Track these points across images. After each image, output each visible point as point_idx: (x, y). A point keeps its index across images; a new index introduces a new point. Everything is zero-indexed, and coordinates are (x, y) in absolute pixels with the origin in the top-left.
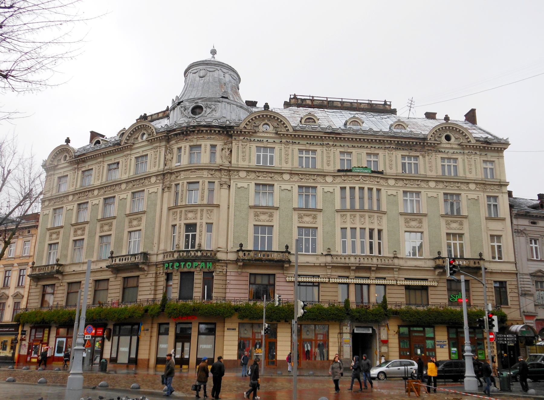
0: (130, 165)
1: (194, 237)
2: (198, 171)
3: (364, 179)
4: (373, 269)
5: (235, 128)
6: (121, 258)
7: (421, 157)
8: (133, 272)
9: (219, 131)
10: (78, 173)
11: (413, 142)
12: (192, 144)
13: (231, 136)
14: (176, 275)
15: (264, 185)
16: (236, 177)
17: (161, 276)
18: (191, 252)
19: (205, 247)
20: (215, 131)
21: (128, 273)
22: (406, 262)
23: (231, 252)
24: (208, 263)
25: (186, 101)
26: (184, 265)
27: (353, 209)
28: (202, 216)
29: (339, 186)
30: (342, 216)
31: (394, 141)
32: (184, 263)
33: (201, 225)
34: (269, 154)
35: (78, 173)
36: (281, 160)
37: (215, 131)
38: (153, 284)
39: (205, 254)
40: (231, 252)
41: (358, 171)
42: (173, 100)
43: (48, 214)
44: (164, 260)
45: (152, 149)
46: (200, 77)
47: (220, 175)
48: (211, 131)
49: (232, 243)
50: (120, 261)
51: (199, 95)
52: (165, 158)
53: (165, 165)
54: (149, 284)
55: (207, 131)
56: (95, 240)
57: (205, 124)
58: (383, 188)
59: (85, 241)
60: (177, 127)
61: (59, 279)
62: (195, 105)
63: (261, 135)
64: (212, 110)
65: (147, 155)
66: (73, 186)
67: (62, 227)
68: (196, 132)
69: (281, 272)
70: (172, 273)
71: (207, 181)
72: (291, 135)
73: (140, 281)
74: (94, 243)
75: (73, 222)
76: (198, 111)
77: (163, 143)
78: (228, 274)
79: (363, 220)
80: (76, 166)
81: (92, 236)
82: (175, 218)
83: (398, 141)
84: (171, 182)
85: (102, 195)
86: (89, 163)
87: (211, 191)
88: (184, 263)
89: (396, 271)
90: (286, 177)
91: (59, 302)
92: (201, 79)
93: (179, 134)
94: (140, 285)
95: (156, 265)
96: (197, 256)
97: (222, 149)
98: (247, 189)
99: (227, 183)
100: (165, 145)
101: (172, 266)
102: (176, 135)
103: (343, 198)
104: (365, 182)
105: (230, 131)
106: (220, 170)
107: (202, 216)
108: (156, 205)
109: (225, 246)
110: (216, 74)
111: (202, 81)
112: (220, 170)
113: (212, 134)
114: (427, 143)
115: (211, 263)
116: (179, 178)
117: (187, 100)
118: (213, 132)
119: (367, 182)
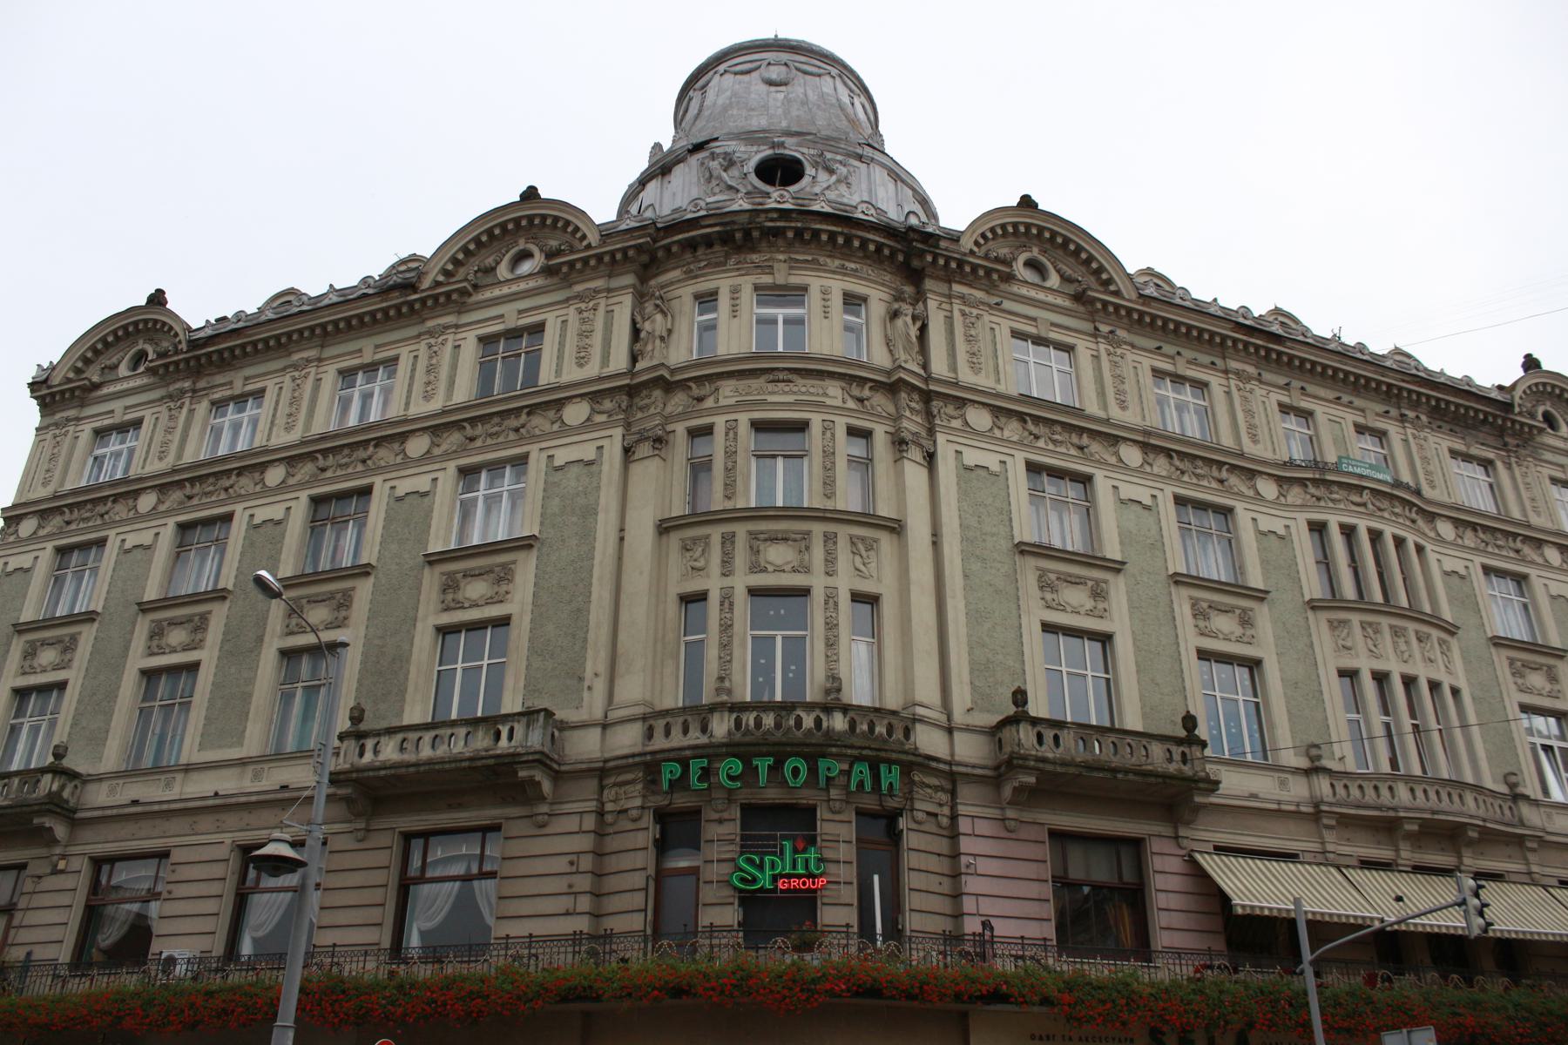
0: (454, 367)
1: (795, 650)
2: (800, 381)
3: (1378, 504)
4: (1473, 834)
5: (943, 244)
6: (413, 736)
7: (1499, 464)
8: (460, 806)
9: (879, 247)
10: (192, 411)
11: (1477, 411)
12: (766, 279)
14: (720, 821)
15: (1058, 474)
16: (956, 423)
19: (859, 692)
20: (864, 243)
22: (1549, 816)
23: (968, 729)
24: (883, 768)
26: (776, 768)
27: (1362, 603)
28: (830, 560)
29: (1302, 518)
30: (1334, 625)
31: (1428, 397)
33: (831, 598)
36: (1102, 393)
38: (586, 863)
39: (865, 727)
40: (968, 729)
41: (1358, 471)
42: (657, 146)
45: (567, 300)
46: (771, 83)
47: (891, 409)
48: (848, 240)
49: (967, 689)
50: (402, 749)
52: (636, 332)
53: (634, 359)
55: (832, 236)
57: (827, 209)
58: (1429, 547)
59: (205, 678)
61: (54, 842)
62: (770, 152)
63: (1024, 291)
64: (839, 181)
65: (538, 329)
66: (160, 459)
67: (89, 617)
68: (790, 234)
69: (1165, 830)
70: (696, 812)
71: (841, 423)
72: (1129, 311)
74: (251, 681)
75: (151, 593)
77: (629, 279)
78: (964, 825)
79: (1403, 647)
80: (187, 384)
81: (239, 650)
83: (1438, 400)
84: (668, 419)
85: (302, 486)
87: (865, 464)
88: (771, 761)
89: (1533, 850)
90: (1132, 455)
92: (773, 89)
93: (708, 242)
95: (602, 772)
96: (829, 733)
97: (895, 315)
98: (998, 477)
99: (924, 442)
100: (634, 286)
101: (706, 774)
102: (691, 245)
103: (1325, 562)
104: (1379, 513)
105: (922, 254)
106: (892, 387)
107: (830, 560)
108: (590, 512)
110: (827, 84)
111: (781, 96)
112: (892, 387)
114: (1514, 422)
115: (896, 769)
116: (709, 403)
118: (856, 243)
119: (1386, 515)
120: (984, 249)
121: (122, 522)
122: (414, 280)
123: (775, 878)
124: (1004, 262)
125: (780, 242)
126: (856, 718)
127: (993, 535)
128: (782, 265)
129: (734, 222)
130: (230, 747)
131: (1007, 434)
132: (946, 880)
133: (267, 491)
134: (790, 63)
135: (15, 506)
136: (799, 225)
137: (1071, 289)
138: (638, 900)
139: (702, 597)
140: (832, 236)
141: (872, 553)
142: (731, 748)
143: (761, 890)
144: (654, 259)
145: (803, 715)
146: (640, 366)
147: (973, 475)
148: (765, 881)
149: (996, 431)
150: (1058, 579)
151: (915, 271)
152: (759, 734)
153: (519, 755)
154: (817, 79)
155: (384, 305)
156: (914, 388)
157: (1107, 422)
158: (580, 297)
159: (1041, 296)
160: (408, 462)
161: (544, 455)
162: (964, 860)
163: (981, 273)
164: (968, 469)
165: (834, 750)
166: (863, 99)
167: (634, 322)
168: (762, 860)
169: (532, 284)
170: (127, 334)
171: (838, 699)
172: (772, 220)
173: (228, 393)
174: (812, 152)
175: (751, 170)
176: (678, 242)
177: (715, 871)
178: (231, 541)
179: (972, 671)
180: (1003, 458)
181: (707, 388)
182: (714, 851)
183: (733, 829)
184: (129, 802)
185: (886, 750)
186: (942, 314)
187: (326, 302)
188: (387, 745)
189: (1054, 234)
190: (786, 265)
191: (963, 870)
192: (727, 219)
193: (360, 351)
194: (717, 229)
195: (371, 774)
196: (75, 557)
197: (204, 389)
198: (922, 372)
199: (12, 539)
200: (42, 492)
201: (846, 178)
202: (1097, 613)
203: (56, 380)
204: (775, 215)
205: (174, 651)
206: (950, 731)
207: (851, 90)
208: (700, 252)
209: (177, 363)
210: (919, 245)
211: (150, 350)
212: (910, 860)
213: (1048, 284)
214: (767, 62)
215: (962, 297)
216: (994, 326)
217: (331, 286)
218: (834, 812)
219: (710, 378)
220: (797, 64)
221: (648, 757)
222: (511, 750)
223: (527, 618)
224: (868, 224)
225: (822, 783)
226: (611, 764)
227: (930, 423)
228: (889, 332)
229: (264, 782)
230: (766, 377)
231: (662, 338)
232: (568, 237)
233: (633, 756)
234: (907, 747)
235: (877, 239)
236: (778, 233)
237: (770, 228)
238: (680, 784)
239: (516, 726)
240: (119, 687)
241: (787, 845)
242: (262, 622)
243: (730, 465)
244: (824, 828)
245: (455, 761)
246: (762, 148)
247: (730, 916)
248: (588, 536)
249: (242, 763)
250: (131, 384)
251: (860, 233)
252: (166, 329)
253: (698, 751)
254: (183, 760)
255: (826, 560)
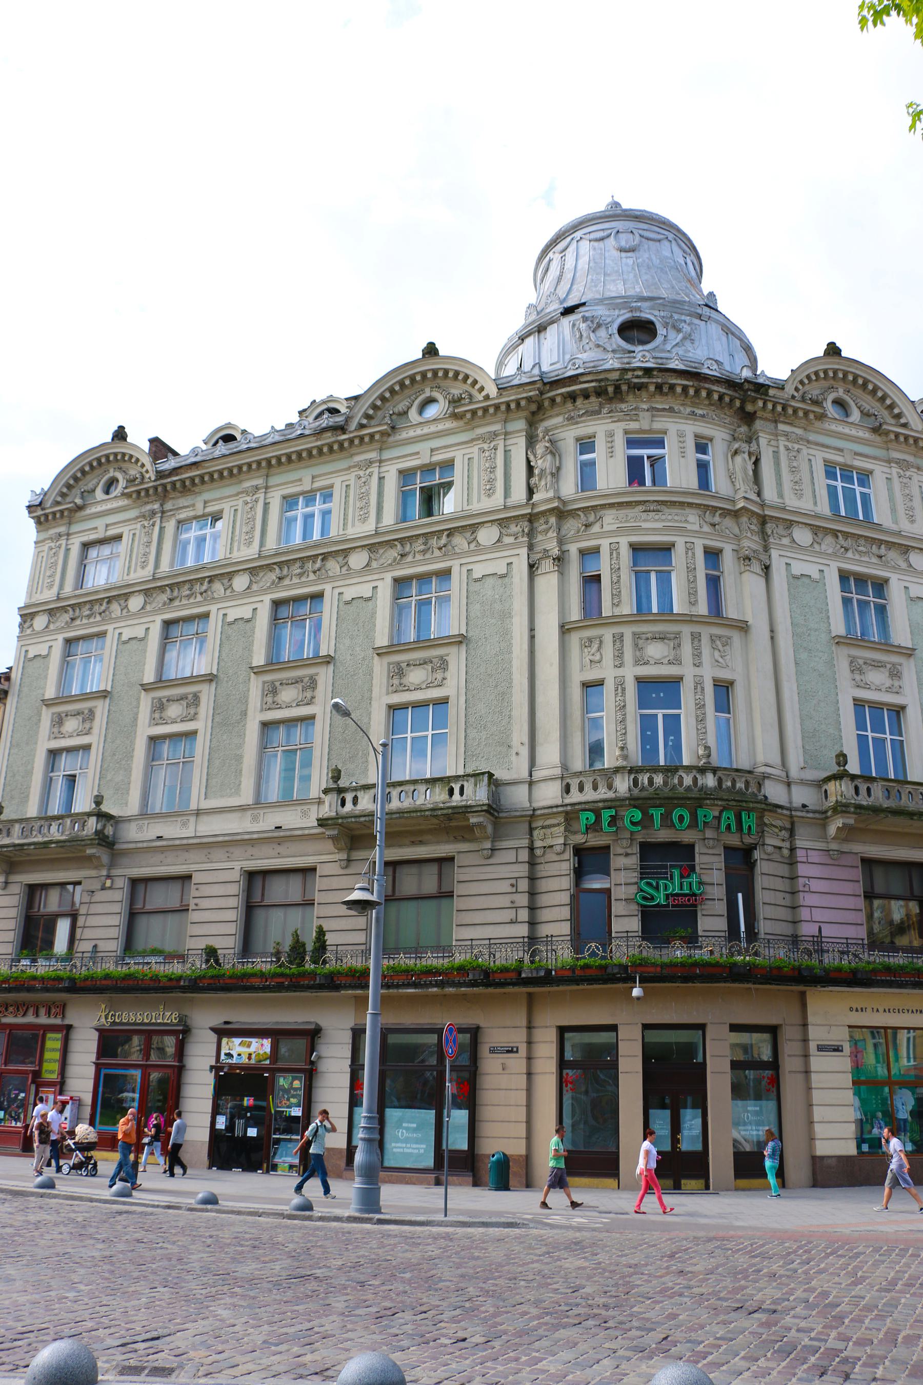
1: (673, 724)
2: (666, 510)
5: (771, 392)
8: (421, 843)
10: (162, 529)
12: (634, 425)
13: (748, 418)
14: (627, 855)
16: (786, 541)
17: (551, 856)
18: (681, 773)
21: (400, 846)
23: (803, 782)
25: (597, 304)
28: (697, 654)
32: (663, 810)
34: (858, 490)
35: (162, 529)
36: (893, 510)
37: (710, 393)
38: (524, 885)
39: (729, 784)
43: (48, 655)
44: (567, 801)
47: (736, 531)
48: (697, 392)
51: (639, 289)
52: (530, 469)
53: (531, 492)
54: (505, 886)
56: (242, 735)
57: (681, 367)
60: (581, 371)
62: (626, 316)
63: (833, 427)
66: (143, 568)
68: (652, 388)
70: (607, 848)
71: (699, 545)
73: (460, 874)
74: (240, 746)
76: (635, 333)
78: (800, 854)
80: (156, 506)
82: (597, 657)
86: (206, 496)
88: (663, 810)
91: (99, 943)
92: (623, 254)
93: (586, 395)
94: (459, 890)
95: (531, 818)
97: (736, 452)
98: (819, 583)
99: (762, 557)
102: (572, 397)
105: (754, 401)
106: (735, 514)
107: (697, 654)
108: (506, 615)
109: (776, 759)
110: (665, 249)
111: (630, 261)
113: (694, 405)
115: (753, 815)
116: (596, 528)
117: (601, 301)
120: (801, 392)
121: (118, 619)
122: (343, 423)
123: (667, 896)
124: (816, 402)
125: (644, 394)
126: (723, 777)
127: (816, 630)
128: (647, 413)
129: (607, 379)
130: (230, 796)
131: (823, 547)
132: (788, 896)
133: (235, 596)
134: (634, 231)
135: (26, 607)
136: (659, 380)
137: (871, 422)
138: (566, 912)
139: (600, 683)
140: (685, 389)
141: (727, 648)
142: (634, 801)
143: (658, 905)
144: (540, 407)
145: (684, 775)
146: (536, 497)
147: (800, 582)
148: (661, 899)
149: (816, 545)
150: (865, 663)
151: (749, 413)
152: (651, 790)
153: (470, 806)
154: (658, 244)
155: (319, 443)
156: (753, 513)
157: (898, 534)
158: (482, 438)
159: (847, 430)
160: (350, 573)
161: (464, 569)
162: (801, 881)
163: (801, 414)
164: (796, 578)
165: (708, 802)
166: (693, 257)
167: (528, 461)
168: (657, 883)
169: (441, 427)
170: (100, 464)
171: (709, 763)
172: (637, 377)
173: (192, 514)
174: (662, 314)
175: (616, 331)
176: (562, 394)
177: (619, 893)
178: (210, 634)
179: (803, 738)
180: (822, 567)
181: (592, 518)
182: (619, 877)
183: (634, 861)
184: (154, 838)
185: (746, 802)
186: (771, 449)
187: (270, 440)
188: (363, 798)
189: (856, 377)
190: (648, 414)
191: (801, 889)
192: (602, 376)
193: (300, 480)
194: (593, 384)
195: (353, 820)
196: (81, 647)
197: (171, 510)
198: (757, 499)
199: (29, 631)
200: (49, 595)
201: (690, 335)
202: (895, 690)
203: (48, 504)
204: (640, 373)
205: (174, 722)
206: (789, 784)
207: (684, 252)
208: (579, 401)
209: (147, 490)
210: (753, 394)
211: (119, 476)
212: (760, 882)
213: (851, 420)
214: (616, 230)
215: (786, 435)
216: (811, 457)
217: (273, 427)
218: (709, 848)
219: (594, 508)
220: (640, 232)
221: (569, 808)
222: (464, 803)
223: (462, 699)
224: (713, 378)
225: (701, 824)
226: (539, 812)
227: (765, 541)
228: (731, 467)
229: (261, 823)
230: (641, 508)
231: (552, 474)
232: (467, 387)
233: (557, 806)
234: (760, 797)
235: (720, 390)
236: (640, 387)
237: (635, 383)
238: (595, 827)
239: (465, 784)
240: (133, 750)
241: (676, 873)
242: (245, 700)
243: (615, 579)
244: (699, 859)
245: (421, 811)
246: (622, 312)
247: (634, 925)
248: (506, 634)
249: (242, 809)
250: (109, 506)
251: (707, 385)
252: (126, 458)
253: (609, 804)
254: (193, 806)
255: (693, 655)
